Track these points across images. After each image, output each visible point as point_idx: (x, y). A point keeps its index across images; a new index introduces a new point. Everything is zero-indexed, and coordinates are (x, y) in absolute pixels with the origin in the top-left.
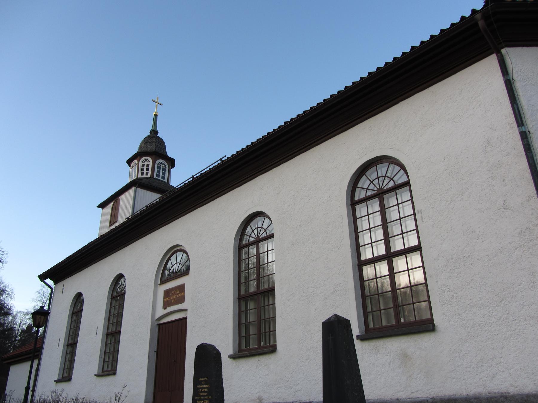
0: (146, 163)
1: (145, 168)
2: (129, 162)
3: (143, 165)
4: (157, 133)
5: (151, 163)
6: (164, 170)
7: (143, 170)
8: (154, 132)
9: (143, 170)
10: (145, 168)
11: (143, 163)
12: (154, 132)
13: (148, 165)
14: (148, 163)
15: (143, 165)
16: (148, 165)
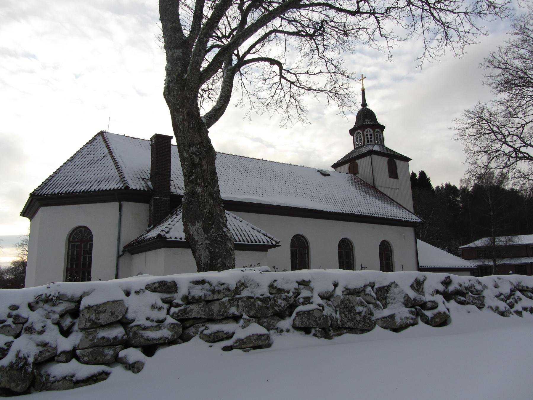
0: (369, 133)
1: (369, 136)
2: (352, 132)
3: (367, 135)
4: (367, 105)
5: (372, 133)
6: (380, 136)
7: (368, 138)
8: (364, 104)
9: (368, 138)
10: (369, 136)
11: (367, 133)
12: (364, 104)
13: (371, 135)
14: (370, 133)
15: (367, 135)
16: (371, 135)
